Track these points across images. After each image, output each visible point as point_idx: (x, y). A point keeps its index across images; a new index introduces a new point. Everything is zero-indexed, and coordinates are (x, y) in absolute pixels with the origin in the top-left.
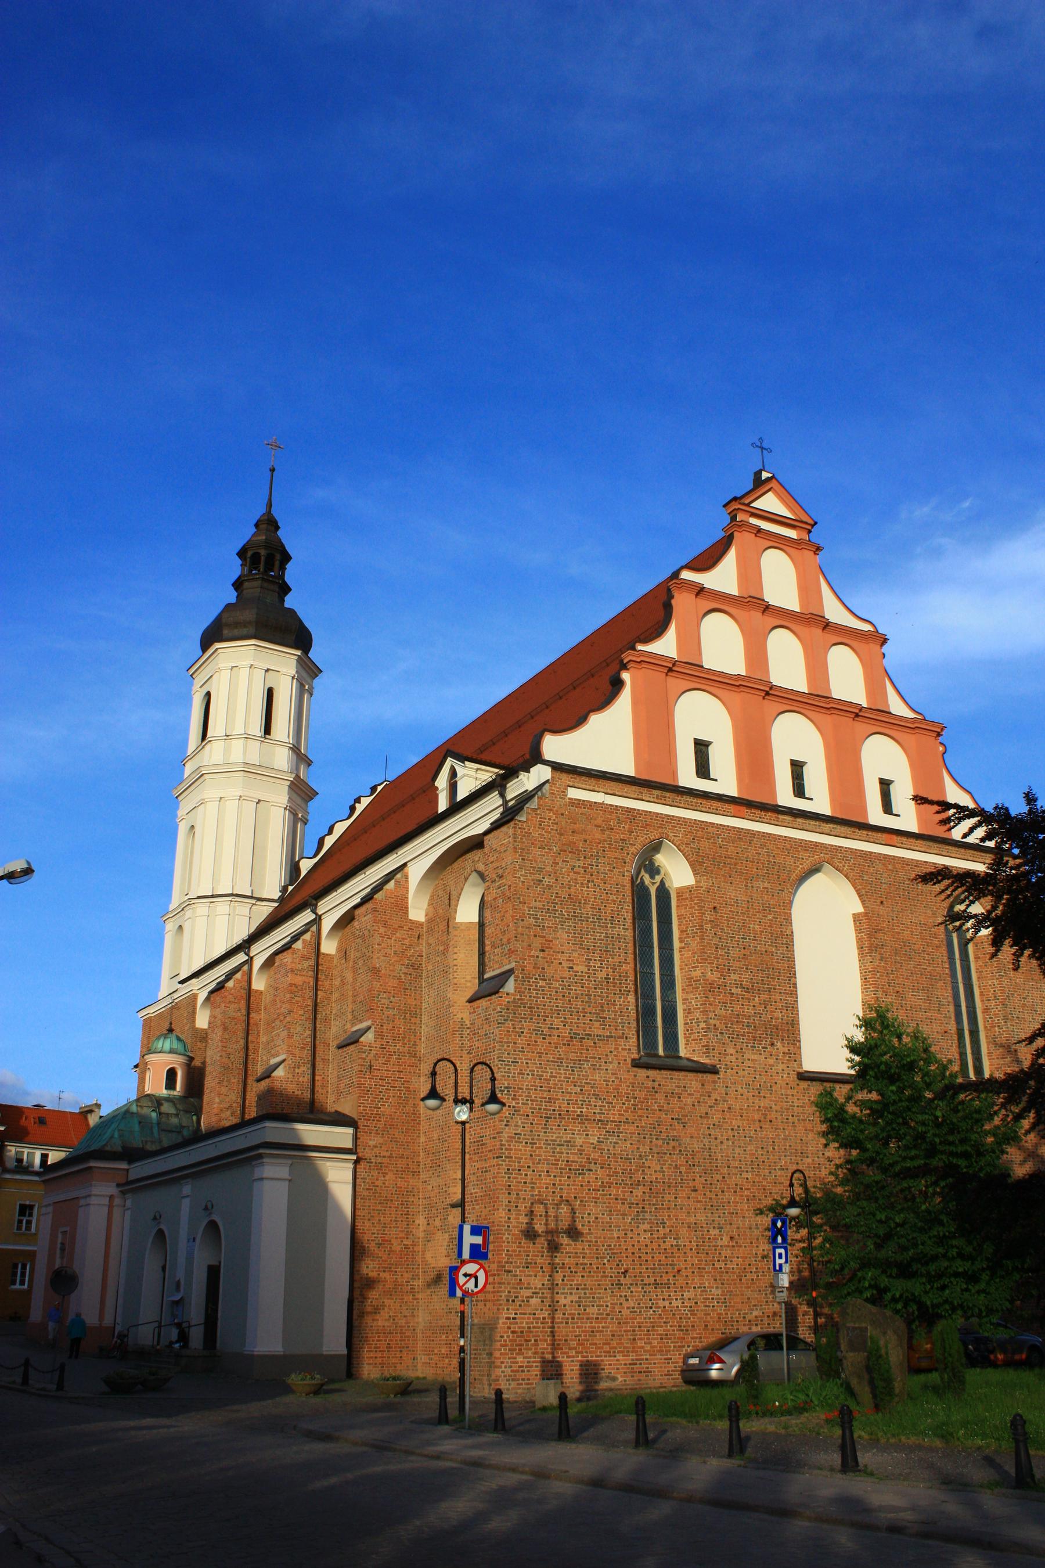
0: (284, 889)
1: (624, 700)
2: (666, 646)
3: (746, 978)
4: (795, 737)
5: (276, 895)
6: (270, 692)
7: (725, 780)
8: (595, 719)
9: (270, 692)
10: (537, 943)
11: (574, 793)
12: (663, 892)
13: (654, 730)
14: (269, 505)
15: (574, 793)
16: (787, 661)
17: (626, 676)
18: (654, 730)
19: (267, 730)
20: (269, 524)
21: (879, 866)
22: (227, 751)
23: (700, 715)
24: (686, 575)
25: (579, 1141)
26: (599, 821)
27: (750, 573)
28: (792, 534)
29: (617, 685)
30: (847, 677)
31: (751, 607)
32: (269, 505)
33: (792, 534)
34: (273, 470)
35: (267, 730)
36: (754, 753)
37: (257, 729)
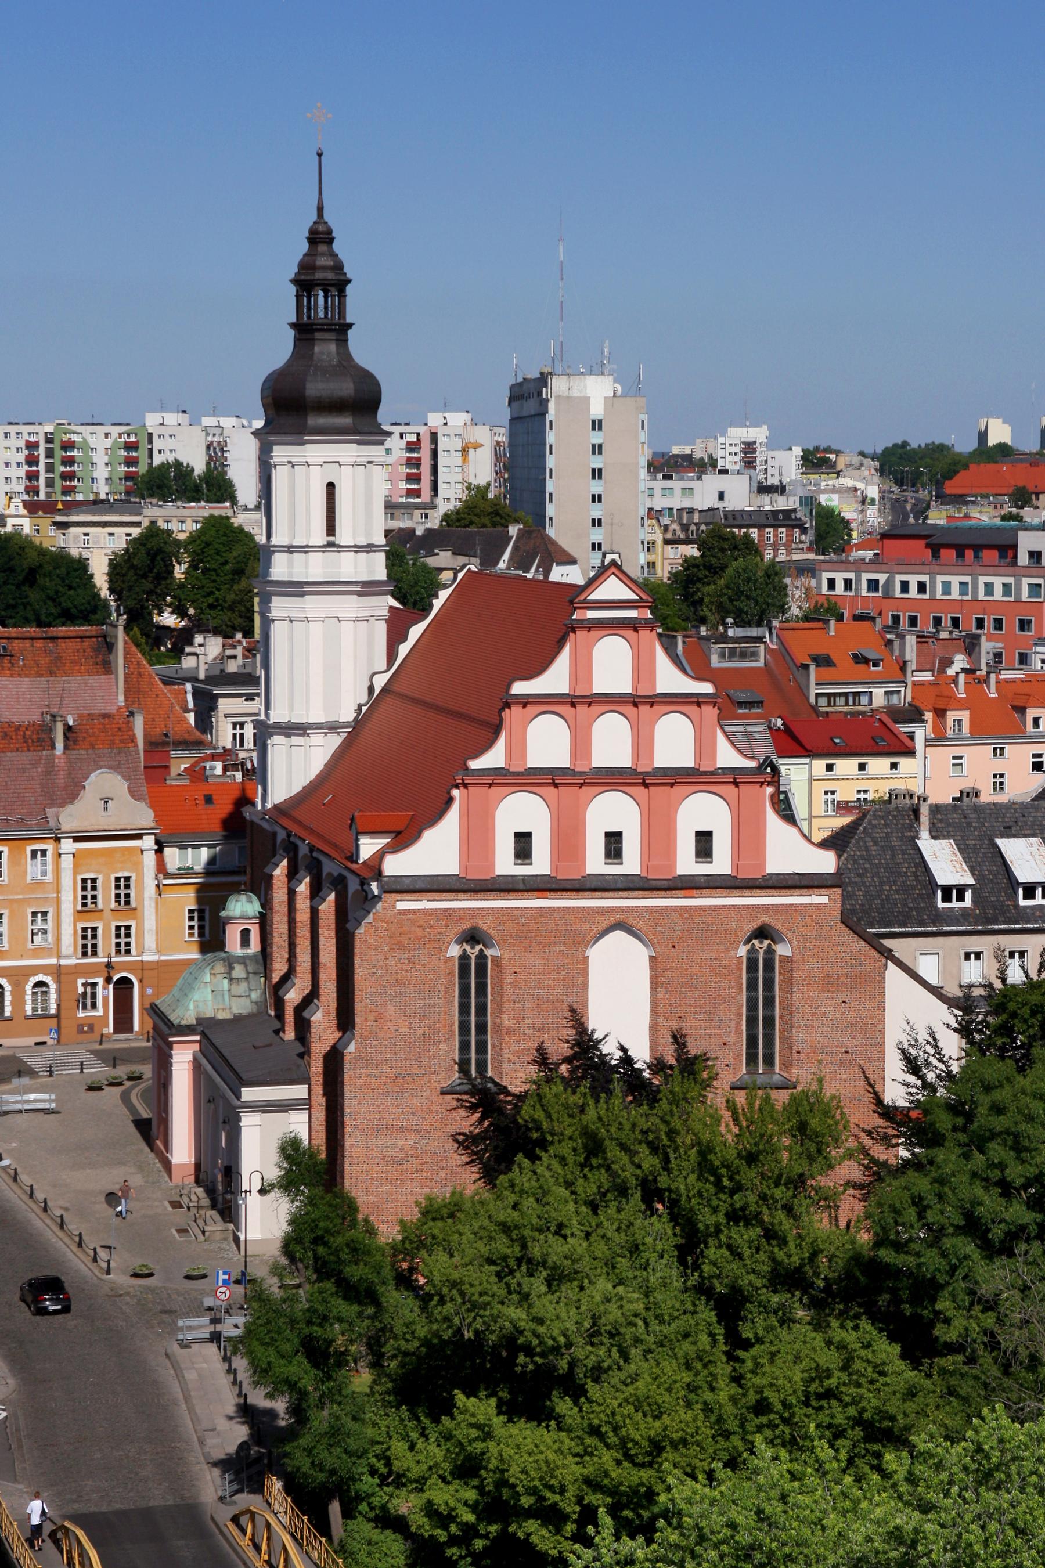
0: (360, 707)
1: (453, 817)
2: (494, 758)
3: (538, 1022)
4: (613, 811)
5: (348, 715)
6: (331, 486)
8: (428, 835)
9: (331, 486)
10: (371, 1017)
11: (401, 905)
12: (481, 956)
13: (477, 837)
14: (320, 210)
15: (401, 905)
16: (611, 742)
17: (456, 793)
18: (477, 837)
19: (331, 530)
20: (320, 237)
21: (675, 916)
22: (291, 564)
23: (523, 811)
24: (519, 688)
25: (400, 1143)
26: (421, 922)
27: (581, 669)
28: (633, 614)
29: (450, 800)
32: (320, 210)
33: (633, 614)
34: (320, 155)
35: (331, 530)
36: (568, 837)
37: (319, 538)
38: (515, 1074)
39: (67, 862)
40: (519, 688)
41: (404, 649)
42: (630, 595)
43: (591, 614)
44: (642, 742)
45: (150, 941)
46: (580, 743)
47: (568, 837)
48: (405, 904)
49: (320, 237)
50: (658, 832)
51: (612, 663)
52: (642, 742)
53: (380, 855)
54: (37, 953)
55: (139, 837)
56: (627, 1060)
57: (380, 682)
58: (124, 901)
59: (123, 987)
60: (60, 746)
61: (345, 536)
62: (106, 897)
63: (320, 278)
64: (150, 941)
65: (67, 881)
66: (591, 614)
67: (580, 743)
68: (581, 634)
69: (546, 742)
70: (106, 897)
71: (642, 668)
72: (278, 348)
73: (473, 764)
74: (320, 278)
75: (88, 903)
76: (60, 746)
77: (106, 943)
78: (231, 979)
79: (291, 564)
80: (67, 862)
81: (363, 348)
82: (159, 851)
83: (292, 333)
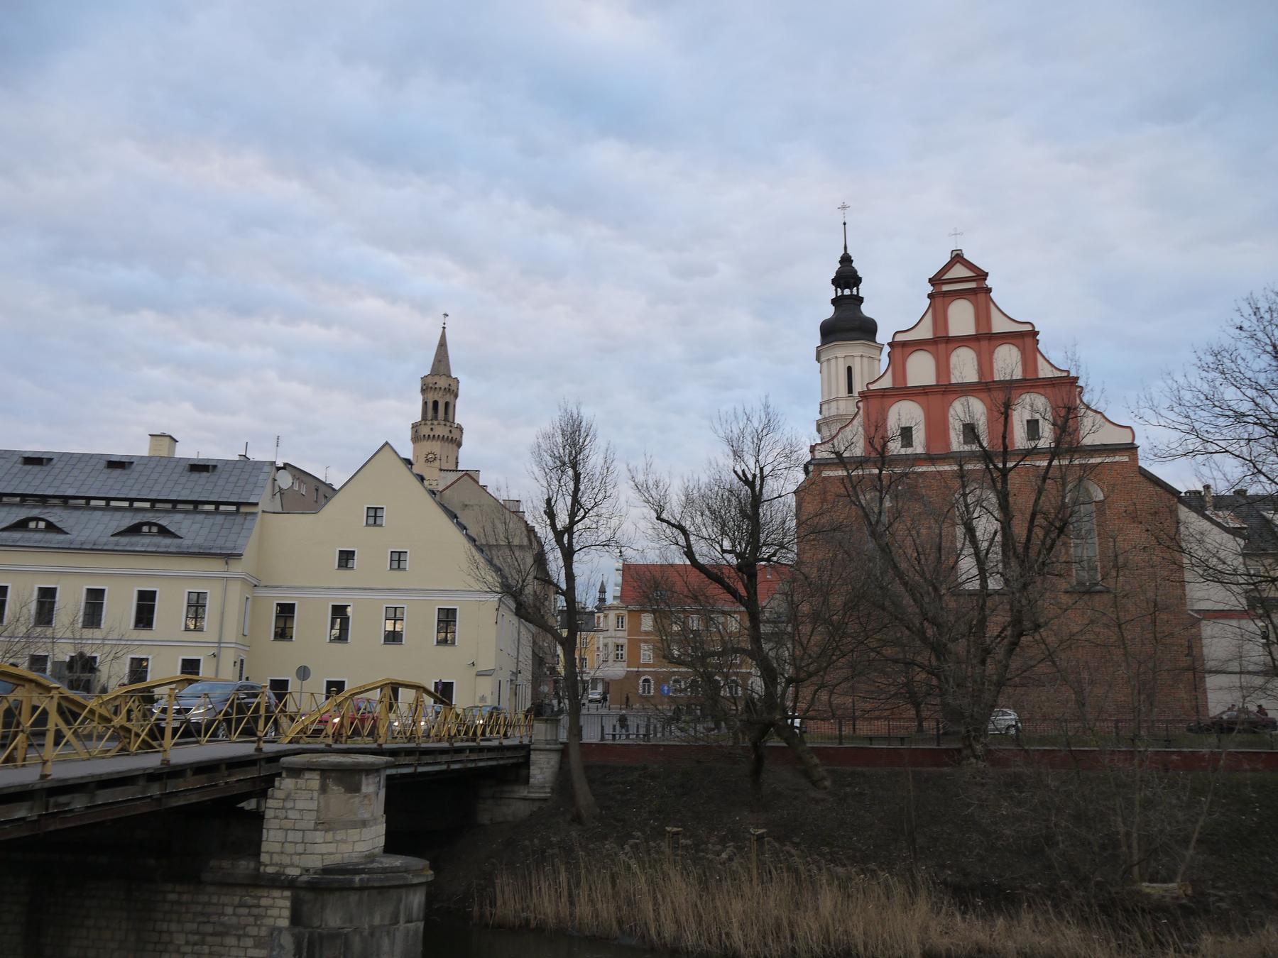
6: (849, 369)
7: (919, 447)
9: (849, 369)
14: (846, 248)
16: (964, 366)
17: (860, 404)
20: (846, 260)
30: (1007, 362)
31: (941, 343)
32: (846, 248)
33: (972, 285)
42: (969, 274)
43: (946, 288)
46: (943, 367)
47: (937, 427)
49: (846, 260)
52: (985, 364)
63: (847, 277)
66: (946, 288)
67: (943, 367)
68: (939, 300)
74: (847, 277)
81: (867, 310)
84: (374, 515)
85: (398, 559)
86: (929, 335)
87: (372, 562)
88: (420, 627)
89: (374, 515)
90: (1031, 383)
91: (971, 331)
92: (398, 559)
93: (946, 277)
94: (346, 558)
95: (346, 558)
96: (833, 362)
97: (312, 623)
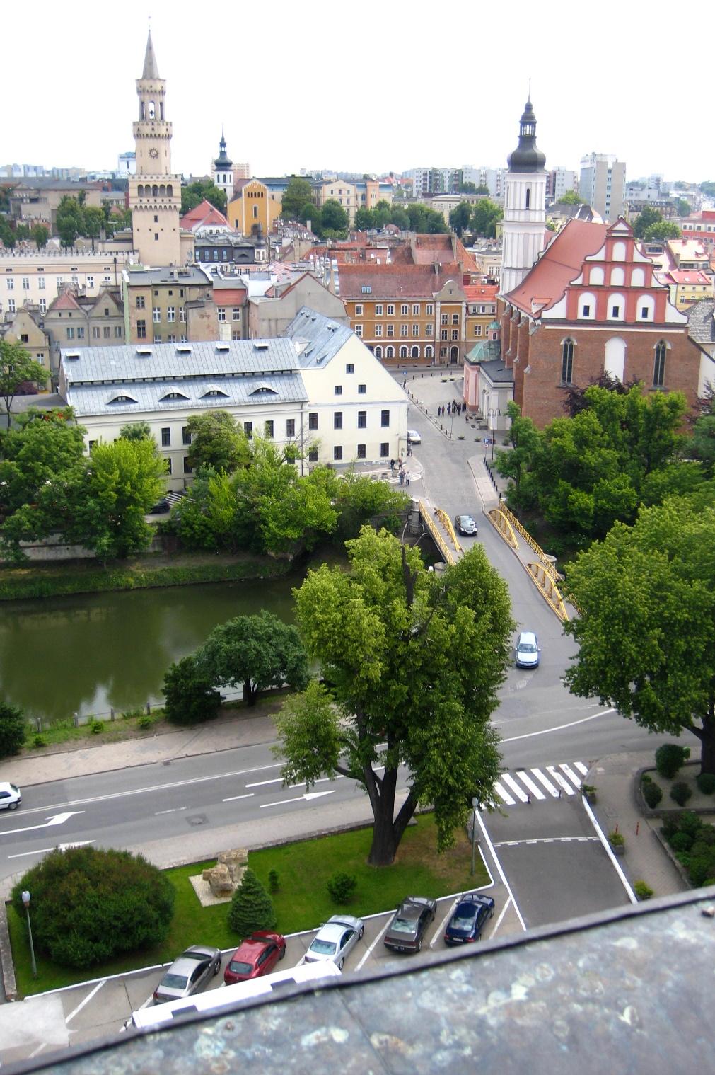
1: (565, 300)
4: (616, 300)
5: (530, 265)
6: (528, 191)
9: (528, 191)
12: (571, 345)
13: (572, 306)
15: (547, 327)
16: (617, 277)
18: (572, 306)
19: (528, 204)
20: (529, 107)
22: (514, 216)
23: (587, 299)
27: (609, 253)
31: (608, 264)
33: (626, 235)
35: (528, 204)
36: (601, 308)
37: (523, 207)
38: (580, 381)
39: (438, 310)
40: (588, 259)
41: (550, 245)
42: (626, 229)
44: (628, 277)
45: (463, 336)
46: (607, 277)
47: (601, 308)
48: (547, 327)
49: (529, 107)
50: (631, 307)
51: (619, 252)
52: (628, 277)
53: (540, 311)
54: (428, 338)
55: (461, 302)
56: (617, 379)
57: (541, 255)
58: (455, 323)
59: (455, 350)
60: (437, 272)
61: (532, 207)
62: (450, 322)
64: (463, 336)
65: (438, 316)
66: (614, 235)
67: (607, 277)
68: (609, 242)
69: (597, 277)
70: (450, 322)
71: (629, 253)
72: (513, 145)
73: (572, 283)
75: (444, 323)
76: (437, 272)
77: (449, 336)
78: (490, 349)
79: (514, 216)
80: (438, 310)
81: (541, 147)
82: (467, 308)
83: (518, 139)
84: (350, 368)
85: (362, 389)
86: (603, 259)
87: (350, 392)
88: (374, 418)
89: (350, 368)
90: (645, 290)
91: (623, 259)
92: (362, 389)
93: (616, 228)
94: (338, 390)
95: (338, 390)
96: (518, 185)
97: (326, 421)
